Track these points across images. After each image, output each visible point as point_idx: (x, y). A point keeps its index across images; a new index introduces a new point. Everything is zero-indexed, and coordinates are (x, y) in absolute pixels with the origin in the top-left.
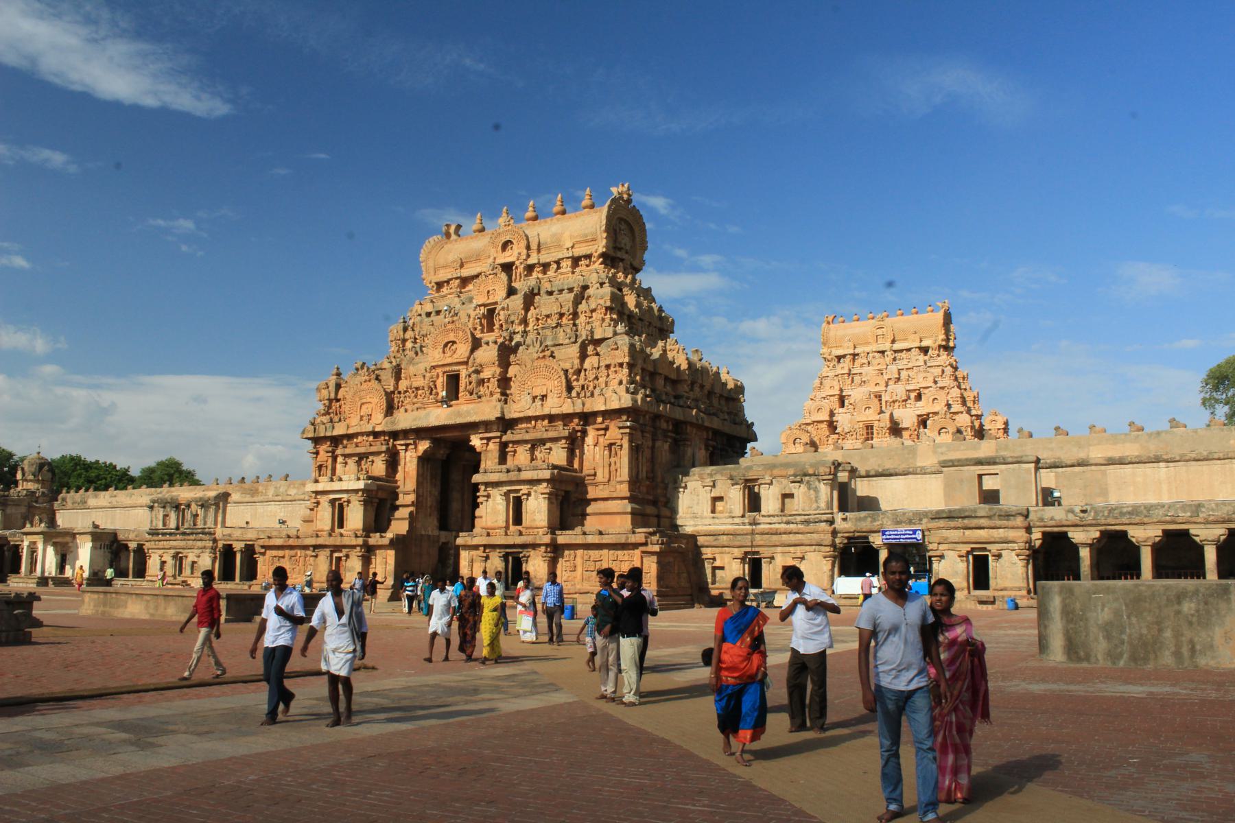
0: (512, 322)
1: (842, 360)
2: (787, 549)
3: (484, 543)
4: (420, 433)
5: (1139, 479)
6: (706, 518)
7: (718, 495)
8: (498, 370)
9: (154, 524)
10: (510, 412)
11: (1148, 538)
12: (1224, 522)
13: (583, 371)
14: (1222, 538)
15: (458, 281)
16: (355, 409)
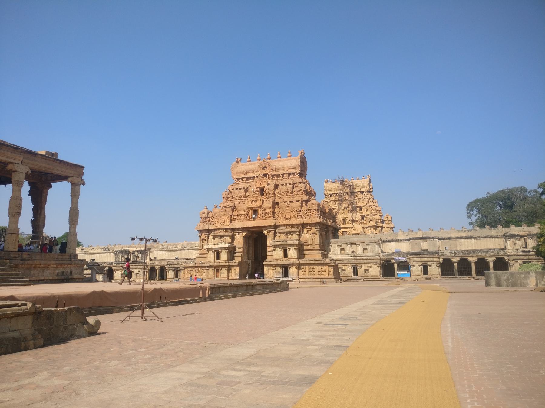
0: (270, 194)
1: (332, 196)
2: (366, 264)
3: (275, 263)
4: (244, 229)
5: (466, 243)
6: (339, 255)
7: (342, 248)
8: (272, 210)
9: (117, 260)
10: (278, 223)
11: (474, 260)
12: (495, 256)
13: (301, 211)
14: (494, 260)
15: (246, 179)
16: (218, 221)
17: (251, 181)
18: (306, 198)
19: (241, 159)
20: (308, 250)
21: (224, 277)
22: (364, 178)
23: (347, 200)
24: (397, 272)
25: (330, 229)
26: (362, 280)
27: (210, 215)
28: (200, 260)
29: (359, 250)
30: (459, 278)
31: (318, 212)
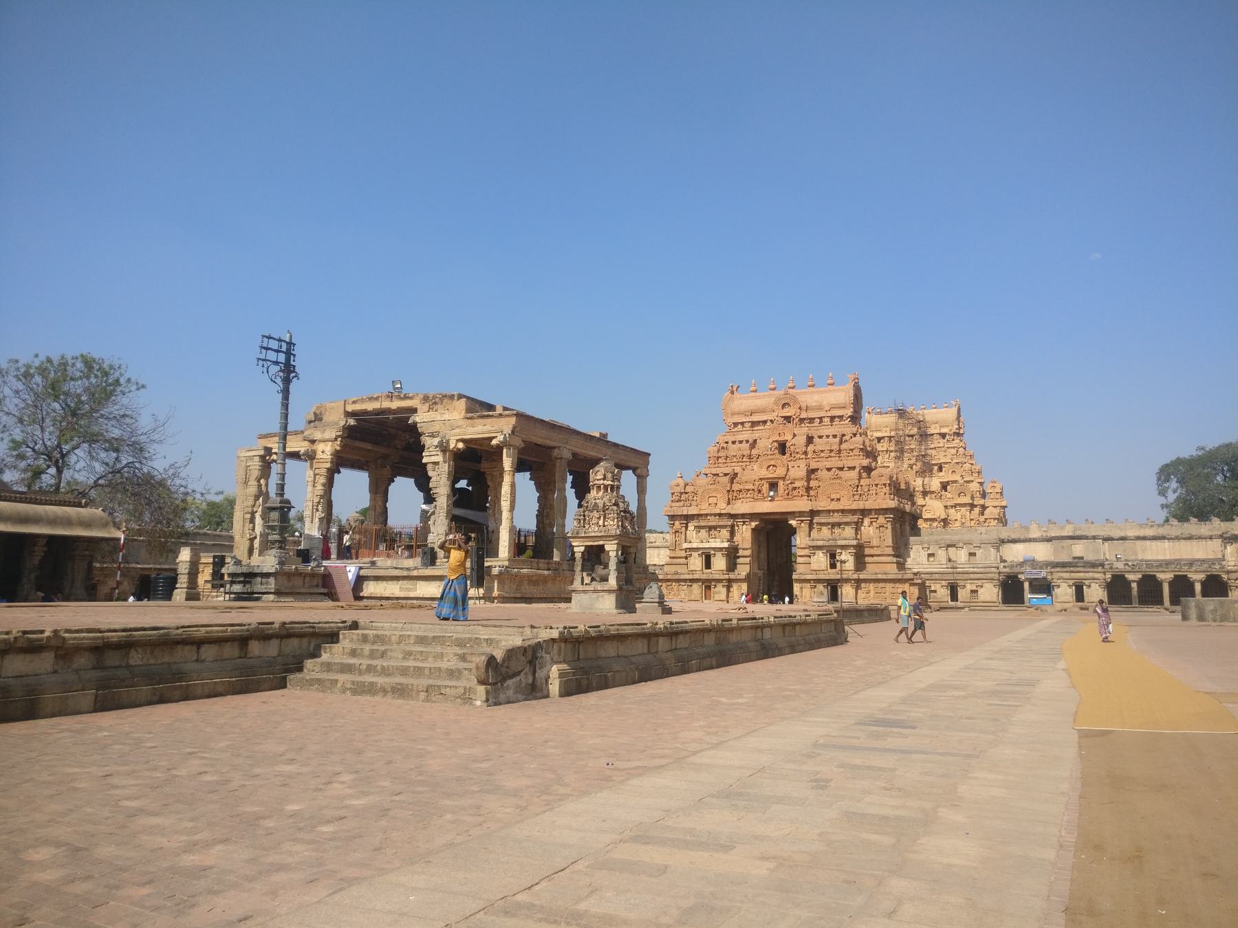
0: (798, 453)
1: (882, 441)
7: (931, 552)
12: (1205, 572)
14: (1204, 579)
15: (750, 424)
17: (759, 428)
18: (865, 462)
19: (739, 386)
20: (872, 556)
21: (721, 599)
22: (947, 407)
23: (912, 450)
24: (1029, 596)
25: (908, 518)
26: (967, 609)
27: (689, 489)
28: (673, 569)
29: (961, 556)
30: (1139, 609)
31: (891, 489)
